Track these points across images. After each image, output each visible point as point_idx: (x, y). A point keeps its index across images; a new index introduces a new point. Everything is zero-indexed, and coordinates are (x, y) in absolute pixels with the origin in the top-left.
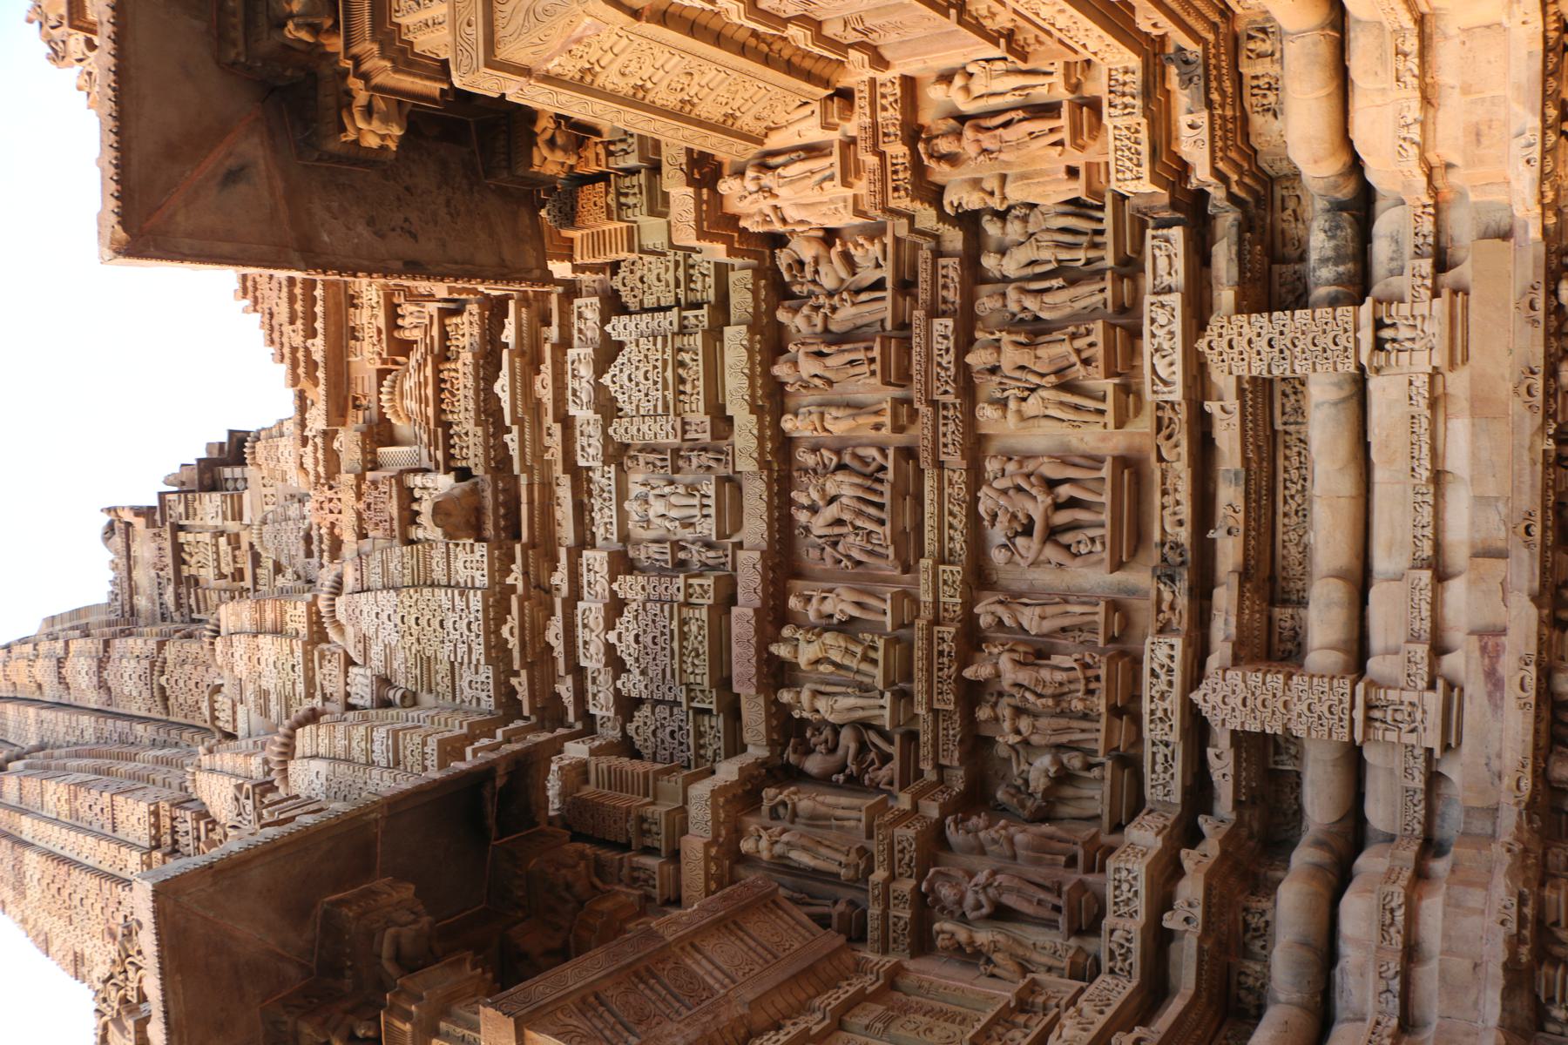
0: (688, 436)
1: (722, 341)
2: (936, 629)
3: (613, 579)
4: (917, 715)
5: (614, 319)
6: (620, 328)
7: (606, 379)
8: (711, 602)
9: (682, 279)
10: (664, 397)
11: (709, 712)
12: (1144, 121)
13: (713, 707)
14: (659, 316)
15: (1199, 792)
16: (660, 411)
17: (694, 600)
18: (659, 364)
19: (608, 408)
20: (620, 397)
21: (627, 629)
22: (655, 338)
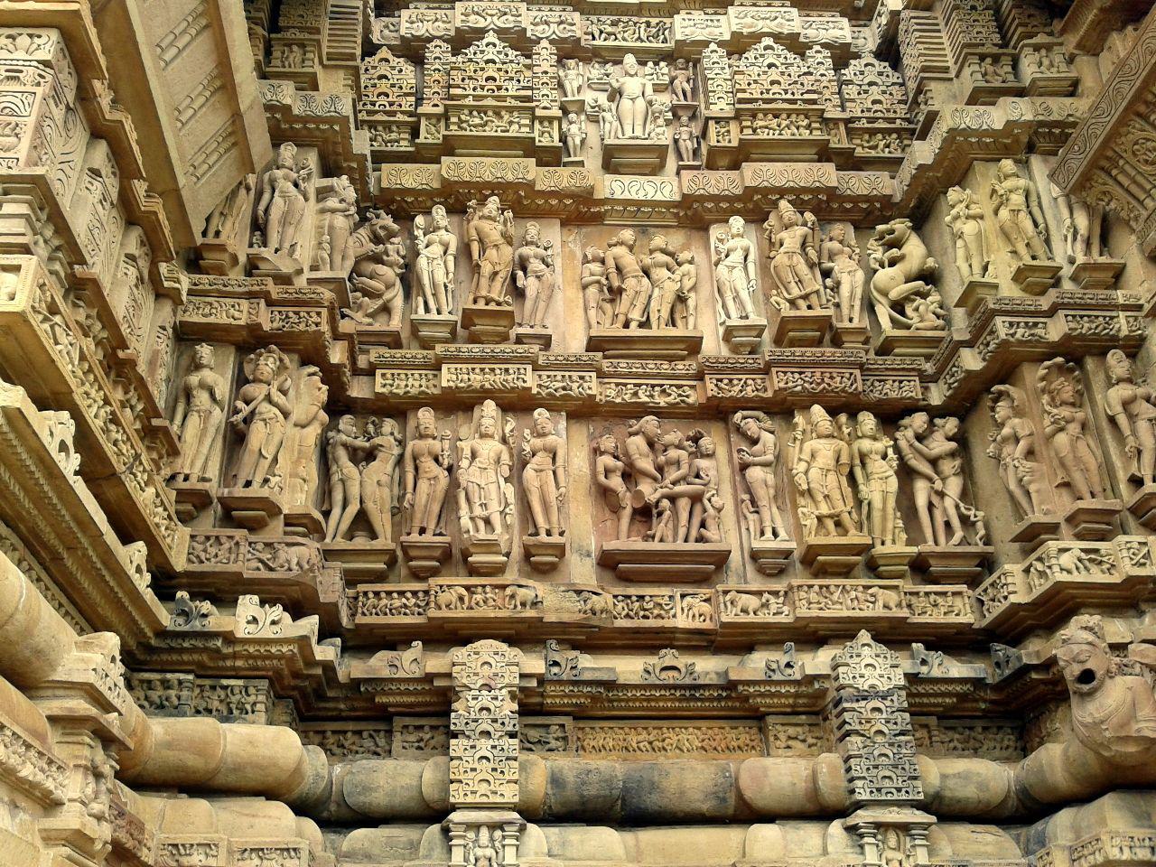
0: (711, 123)
1: (819, 161)
2: (529, 368)
3: (552, 42)
4: (433, 348)
5: (827, 53)
6: (820, 60)
7: (768, 41)
8: (537, 144)
9: (876, 125)
10: (756, 100)
11: (415, 133)
12: (1116, 578)
13: (421, 140)
14: (836, 100)
15: (364, 642)
16: (740, 95)
17: (537, 125)
18: (789, 96)
19: (737, 46)
20: (750, 55)
21: (499, 52)
22: (814, 92)
